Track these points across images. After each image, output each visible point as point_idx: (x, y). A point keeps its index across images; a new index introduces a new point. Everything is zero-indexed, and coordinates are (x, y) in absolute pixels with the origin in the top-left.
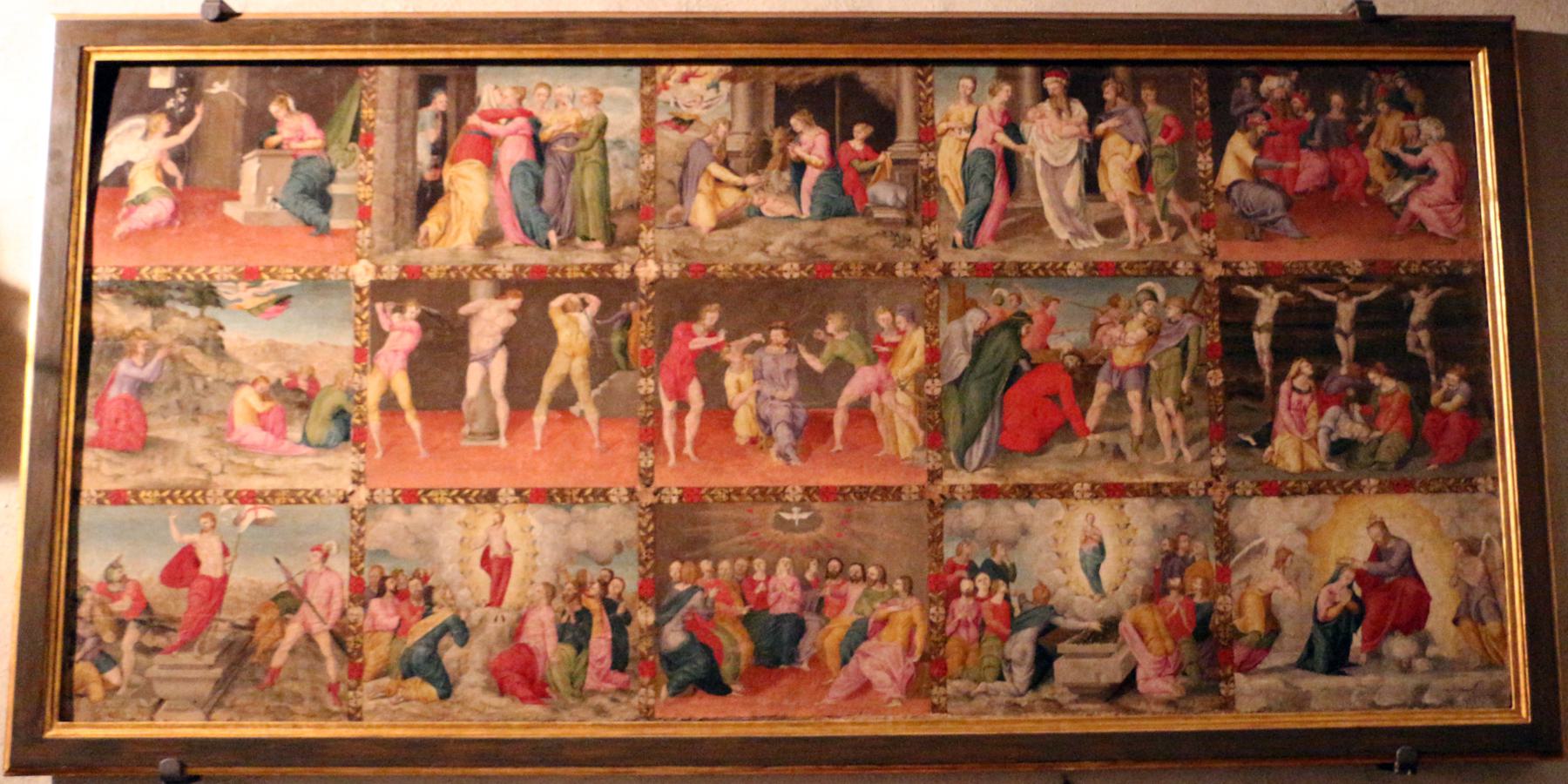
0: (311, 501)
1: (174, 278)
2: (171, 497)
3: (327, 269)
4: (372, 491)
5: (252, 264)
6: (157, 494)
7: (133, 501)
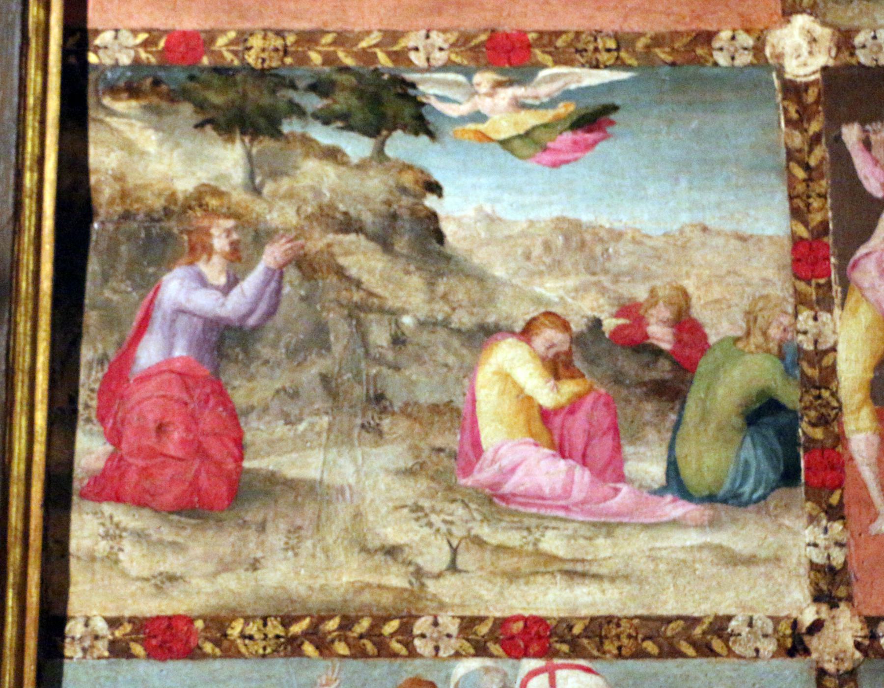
0: (705, 650)
1: (303, 60)
2: (314, 635)
3: (707, 37)
4: (872, 622)
5: (508, 26)
6: (275, 628)
7: (208, 647)
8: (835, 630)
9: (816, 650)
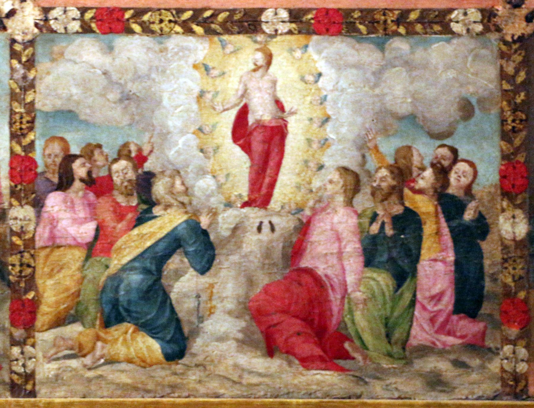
8: (24, 16)
9: (11, 28)
